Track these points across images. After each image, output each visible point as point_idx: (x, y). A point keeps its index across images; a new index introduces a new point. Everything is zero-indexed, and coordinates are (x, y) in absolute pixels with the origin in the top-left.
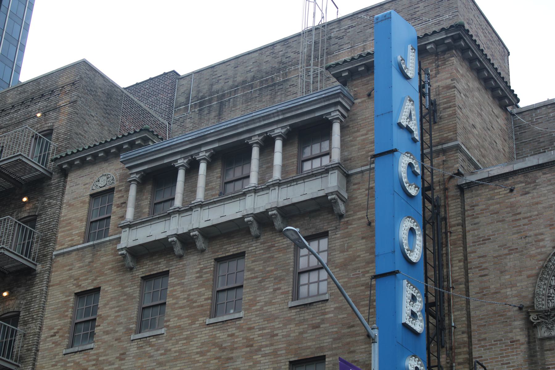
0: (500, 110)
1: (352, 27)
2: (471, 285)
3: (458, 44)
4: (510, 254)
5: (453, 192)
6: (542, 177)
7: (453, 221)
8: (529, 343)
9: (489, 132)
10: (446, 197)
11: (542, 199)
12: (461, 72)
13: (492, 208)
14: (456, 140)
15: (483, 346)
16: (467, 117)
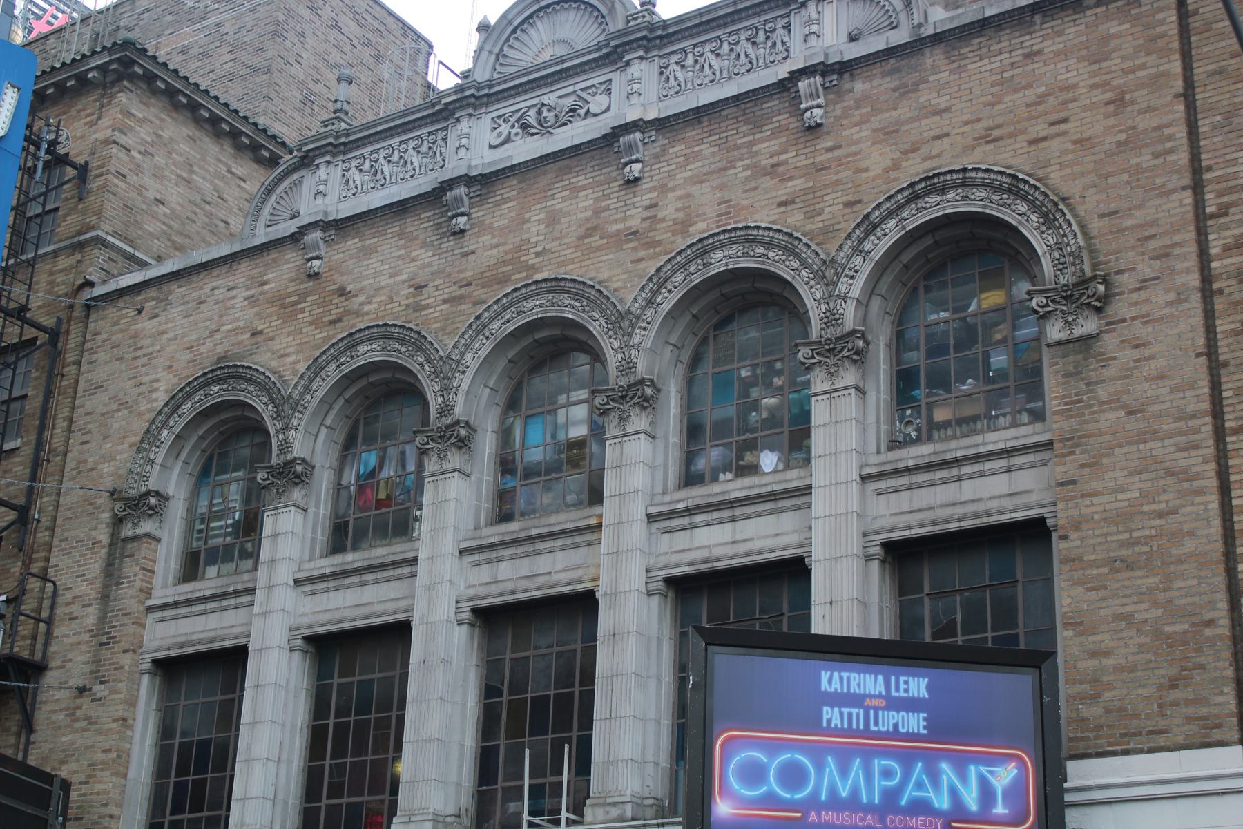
0: (255, 166)
1: (148, 10)
2: (69, 455)
3: (130, 71)
4: (118, 410)
5: (78, 313)
6: (178, 291)
7: (70, 357)
8: (111, 545)
9: (208, 207)
10: (69, 320)
11: (170, 325)
12: (140, 115)
13: (114, 338)
14: (98, 228)
15: (62, 550)
16: (140, 189)
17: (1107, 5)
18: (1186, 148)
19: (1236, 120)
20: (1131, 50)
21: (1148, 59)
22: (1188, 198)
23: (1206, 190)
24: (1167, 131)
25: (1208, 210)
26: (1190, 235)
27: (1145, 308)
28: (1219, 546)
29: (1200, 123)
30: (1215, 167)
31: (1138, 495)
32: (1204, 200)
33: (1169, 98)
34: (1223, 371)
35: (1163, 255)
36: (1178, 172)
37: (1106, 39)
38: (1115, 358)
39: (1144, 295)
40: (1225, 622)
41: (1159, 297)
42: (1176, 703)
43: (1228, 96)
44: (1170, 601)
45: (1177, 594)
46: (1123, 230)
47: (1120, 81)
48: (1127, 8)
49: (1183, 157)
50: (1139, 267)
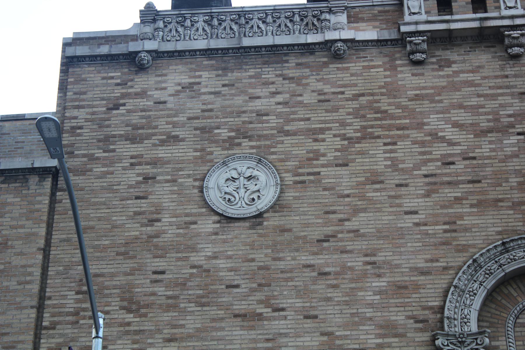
17: (9, 184)
18: (38, 282)
19: (71, 272)
20: (17, 215)
21: (27, 222)
22: (33, 313)
23: (45, 311)
24: (29, 270)
25: (44, 324)
26: (30, 337)
29: (50, 269)
30: (53, 298)
32: (42, 317)
33: (35, 250)
36: (31, 296)
37: (5, 204)
43: (69, 256)
47: (8, 232)
48: (20, 189)
49: (35, 288)
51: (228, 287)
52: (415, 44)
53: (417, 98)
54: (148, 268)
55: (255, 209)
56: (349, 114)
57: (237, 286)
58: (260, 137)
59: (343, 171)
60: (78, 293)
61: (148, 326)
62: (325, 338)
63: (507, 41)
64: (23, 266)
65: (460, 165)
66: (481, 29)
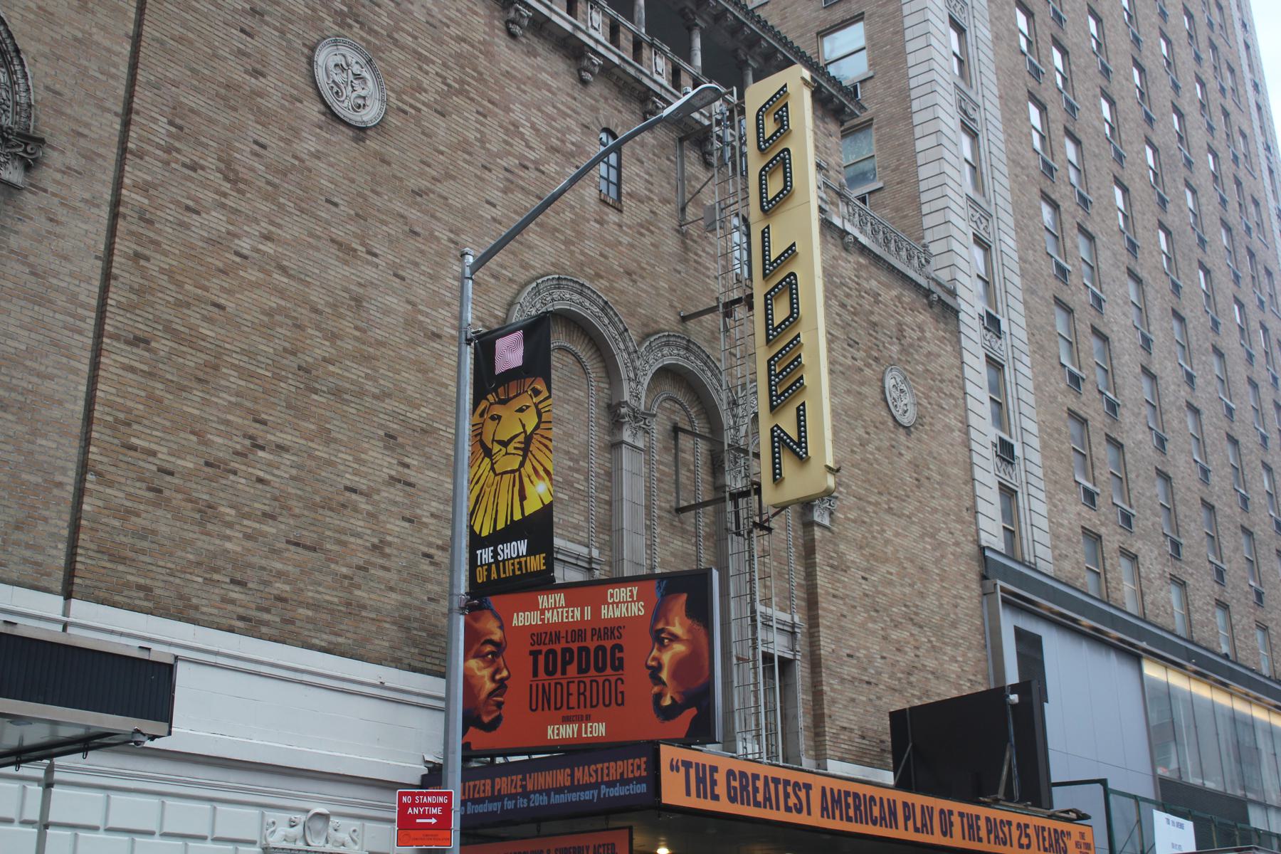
24: (115, 58)
26: (112, 154)
27: (64, 192)
28: (80, 422)
31: (24, 348)
34: (112, 282)
35: (89, 157)
36: (115, 98)
38: (31, 219)
39: (66, 180)
40: (71, 489)
41: (78, 191)
42: (17, 543)
44: (31, 453)
45: (38, 449)
46: (62, 114)
49: (121, 91)
50: (68, 154)
51: (328, 201)
52: (521, 15)
53: (507, 74)
54: (250, 133)
55: (359, 119)
56: (450, 55)
57: (336, 205)
58: (371, 31)
59: (438, 120)
60: (171, 123)
61: (243, 207)
62: (410, 307)
63: (586, 63)
64: (108, 50)
65: (533, 174)
66: (572, 36)
